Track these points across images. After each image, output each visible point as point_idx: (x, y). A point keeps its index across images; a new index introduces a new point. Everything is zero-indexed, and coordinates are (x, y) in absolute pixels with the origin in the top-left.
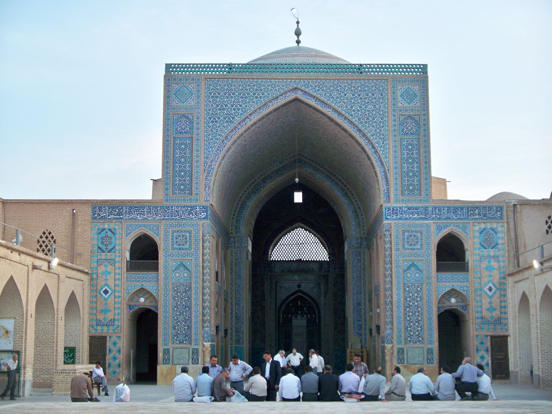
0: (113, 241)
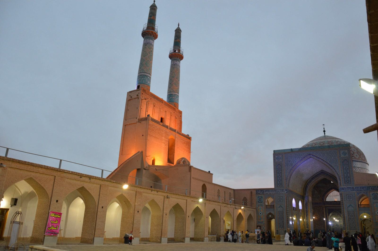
0: (262, 199)
